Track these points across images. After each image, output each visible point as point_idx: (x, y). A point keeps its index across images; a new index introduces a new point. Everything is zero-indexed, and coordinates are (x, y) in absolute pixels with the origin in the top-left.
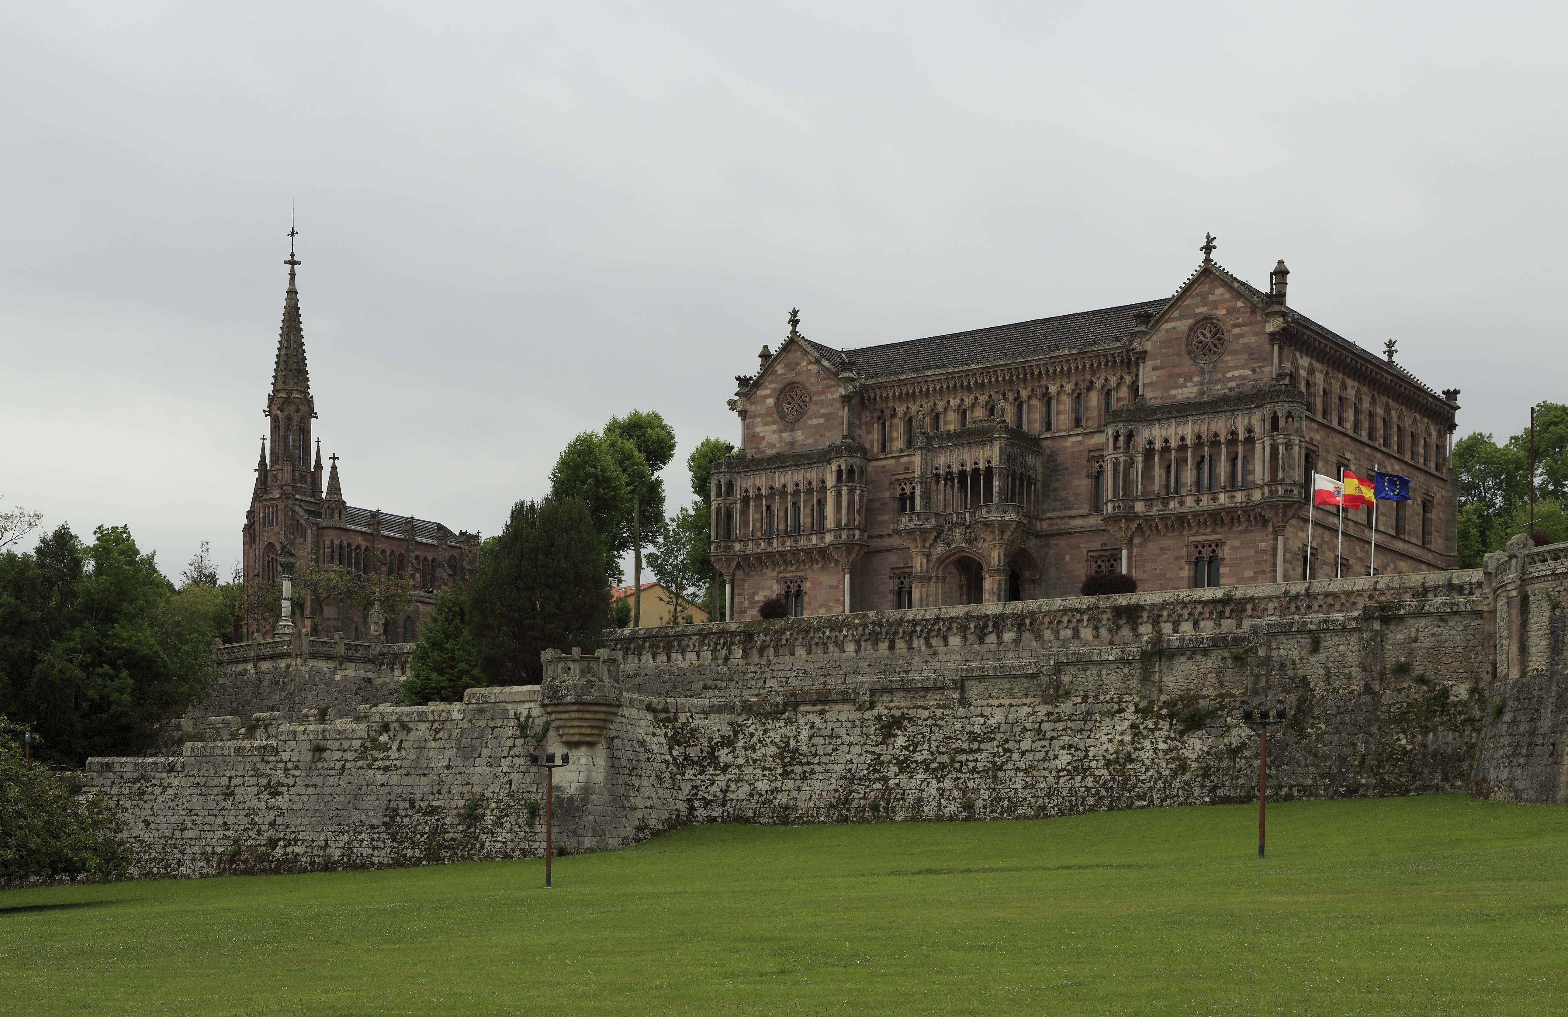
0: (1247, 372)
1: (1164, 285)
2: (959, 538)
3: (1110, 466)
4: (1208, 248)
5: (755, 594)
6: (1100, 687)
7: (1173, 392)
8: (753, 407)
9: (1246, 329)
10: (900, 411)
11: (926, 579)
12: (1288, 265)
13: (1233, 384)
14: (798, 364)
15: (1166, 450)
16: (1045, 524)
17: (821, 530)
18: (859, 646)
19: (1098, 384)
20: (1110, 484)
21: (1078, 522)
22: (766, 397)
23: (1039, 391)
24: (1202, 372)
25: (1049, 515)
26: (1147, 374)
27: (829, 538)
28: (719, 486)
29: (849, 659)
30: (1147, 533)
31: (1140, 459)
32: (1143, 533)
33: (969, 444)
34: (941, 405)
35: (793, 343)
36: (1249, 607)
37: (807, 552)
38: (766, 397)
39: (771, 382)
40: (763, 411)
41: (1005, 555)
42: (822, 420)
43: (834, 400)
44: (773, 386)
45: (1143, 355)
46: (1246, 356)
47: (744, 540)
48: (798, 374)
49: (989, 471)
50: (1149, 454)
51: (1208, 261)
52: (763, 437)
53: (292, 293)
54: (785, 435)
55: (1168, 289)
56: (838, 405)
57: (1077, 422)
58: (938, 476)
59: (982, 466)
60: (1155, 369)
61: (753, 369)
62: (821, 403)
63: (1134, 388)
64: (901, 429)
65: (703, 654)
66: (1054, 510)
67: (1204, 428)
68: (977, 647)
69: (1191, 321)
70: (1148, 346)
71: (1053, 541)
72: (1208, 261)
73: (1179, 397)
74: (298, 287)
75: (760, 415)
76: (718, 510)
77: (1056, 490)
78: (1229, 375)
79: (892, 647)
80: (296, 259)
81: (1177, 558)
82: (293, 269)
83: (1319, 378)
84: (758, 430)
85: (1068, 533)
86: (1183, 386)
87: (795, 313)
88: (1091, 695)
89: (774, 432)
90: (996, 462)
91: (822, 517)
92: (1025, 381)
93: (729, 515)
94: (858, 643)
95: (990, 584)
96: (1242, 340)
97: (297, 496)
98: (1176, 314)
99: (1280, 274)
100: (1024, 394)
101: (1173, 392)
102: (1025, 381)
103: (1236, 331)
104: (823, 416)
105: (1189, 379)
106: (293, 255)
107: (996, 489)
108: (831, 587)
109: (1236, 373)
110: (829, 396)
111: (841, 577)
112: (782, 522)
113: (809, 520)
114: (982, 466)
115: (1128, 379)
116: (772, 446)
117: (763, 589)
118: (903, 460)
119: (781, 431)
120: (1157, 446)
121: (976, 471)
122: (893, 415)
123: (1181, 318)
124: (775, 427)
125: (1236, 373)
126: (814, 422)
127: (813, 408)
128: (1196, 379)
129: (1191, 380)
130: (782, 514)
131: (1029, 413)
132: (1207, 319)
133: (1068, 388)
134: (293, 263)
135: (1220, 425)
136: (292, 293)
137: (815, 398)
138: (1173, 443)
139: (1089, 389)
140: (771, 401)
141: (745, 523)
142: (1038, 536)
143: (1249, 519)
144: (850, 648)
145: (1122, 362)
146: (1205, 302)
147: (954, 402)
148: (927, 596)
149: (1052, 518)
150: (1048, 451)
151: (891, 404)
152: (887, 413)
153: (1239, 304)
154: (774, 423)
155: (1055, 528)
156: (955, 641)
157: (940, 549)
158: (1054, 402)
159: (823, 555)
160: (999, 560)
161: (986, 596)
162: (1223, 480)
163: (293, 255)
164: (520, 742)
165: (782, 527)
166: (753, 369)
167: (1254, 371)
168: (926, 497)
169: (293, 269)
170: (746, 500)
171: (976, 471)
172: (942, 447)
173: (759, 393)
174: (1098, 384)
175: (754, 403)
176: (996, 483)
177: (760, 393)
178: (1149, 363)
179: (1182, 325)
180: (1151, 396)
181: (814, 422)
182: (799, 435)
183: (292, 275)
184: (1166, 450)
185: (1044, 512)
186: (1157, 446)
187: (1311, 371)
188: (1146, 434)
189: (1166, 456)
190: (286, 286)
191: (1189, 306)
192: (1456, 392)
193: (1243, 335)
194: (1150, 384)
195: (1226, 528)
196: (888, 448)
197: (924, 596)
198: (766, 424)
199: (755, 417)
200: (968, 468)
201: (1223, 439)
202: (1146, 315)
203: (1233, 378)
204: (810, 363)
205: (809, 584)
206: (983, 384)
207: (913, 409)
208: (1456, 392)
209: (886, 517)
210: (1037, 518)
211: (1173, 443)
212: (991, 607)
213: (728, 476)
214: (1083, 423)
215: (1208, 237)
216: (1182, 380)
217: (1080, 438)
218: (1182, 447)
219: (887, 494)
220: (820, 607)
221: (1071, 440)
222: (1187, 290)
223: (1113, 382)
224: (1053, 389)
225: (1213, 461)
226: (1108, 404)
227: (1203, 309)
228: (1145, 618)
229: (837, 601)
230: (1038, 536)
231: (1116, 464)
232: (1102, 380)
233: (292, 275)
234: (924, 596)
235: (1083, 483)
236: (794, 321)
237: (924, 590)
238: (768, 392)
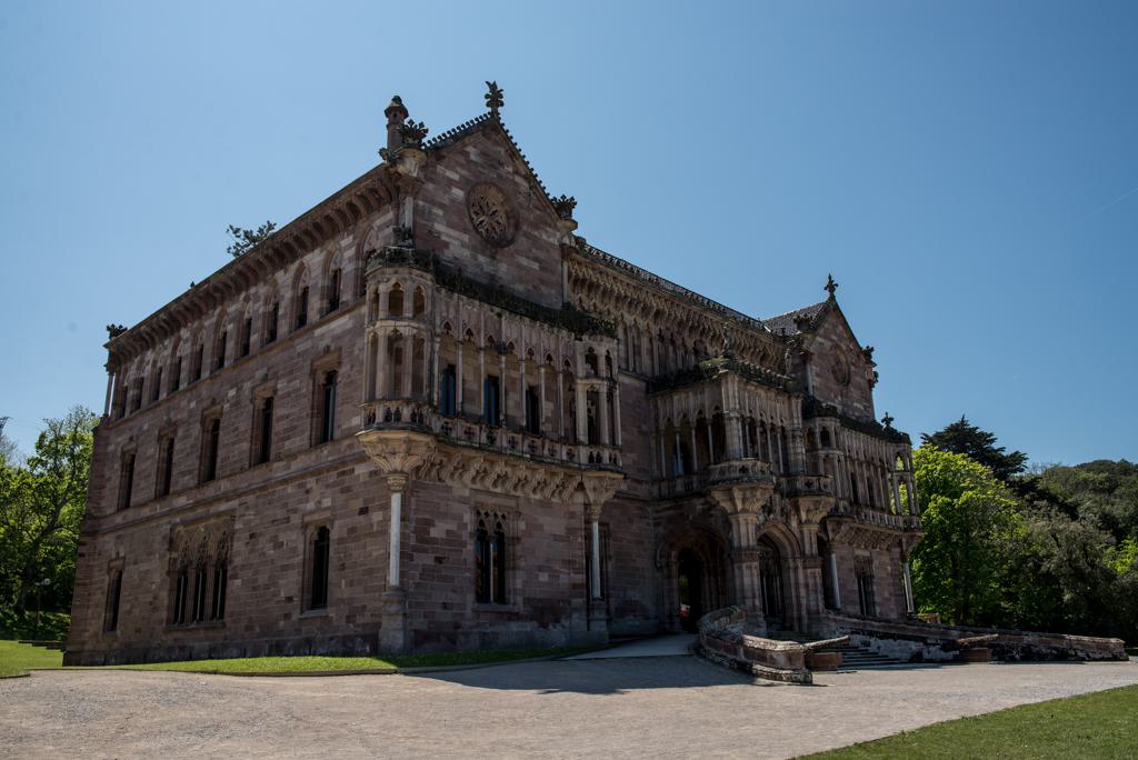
2: (778, 509)
4: (831, 287)
5: (430, 523)
8: (430, 186)
14: (502, 164)
38: (451, 183)
39: (462, 166)
40: (446, 202)
42: (536, 266)
43: (552, 245)
44: (464, 172)
48: (500, 176)
52: (446, 245)
54: (481, 258)
56: (556, 255)
60: (818, 375)
62: (535, 241)
72: (832, 298)
75: (442, 206)
84: (439, 227)
89: (463, 245)
104: (536, 259)
108: (556, 538)
109: (858, 405)
110: (544, 237)
117: (445, 516)
124: (466, 238)
126: (524, 261)
137: (525, 228)
154: (465, 231)
167: (865, 407)
173: (440, 168)
175: (432, 181)
181: (524, 261)
198: (450, 225)
199: (433, 203)
204: (516, 172)
205: (522, 526)
215: (830, 278)
216: (832, 395)
220: (541, 569)
238: (456, 177)
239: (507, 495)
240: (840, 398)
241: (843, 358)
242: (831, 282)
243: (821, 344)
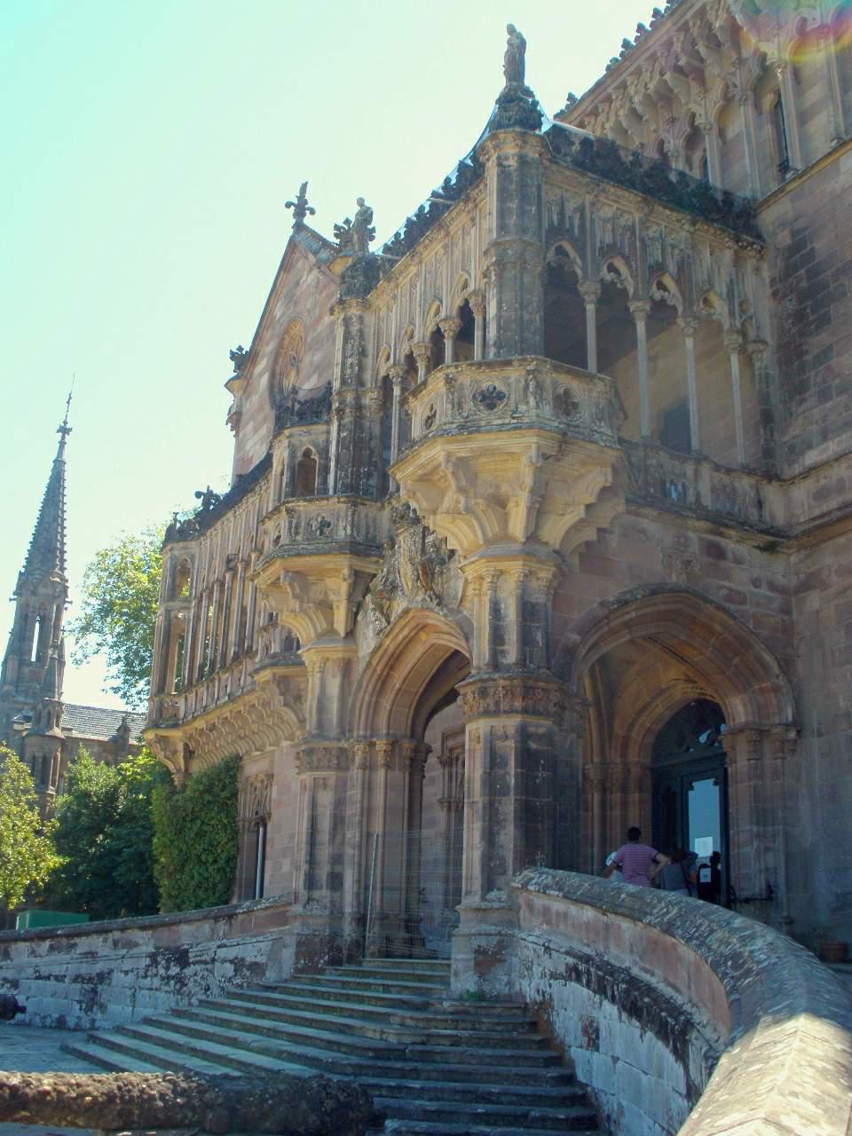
16: (801, 492)
22: (261, 375)
25: (812, 457)
41: (527, 610)
53: (59, 465)
66: (825, 436)
71: (827, 559)
74: (65, 457)
77: (826, 353)
80: (68, 426)
82: (63, 437)
97: (21, 699)
106: (65, 423)
134: (64, 430)
136: (59, 465)
140: (265, 380)
142: (774, 540)
148: (338, 822)
149: (825, 464)
150: (784, 238)
155: (833, 503)
160: (497, 637)
163: (65, 423)
169: (63, 437)
183: (62, 444)
185: (795, 451)
190: (54, 456)
197: (325, 825)
210: (771, 476)
230: (774, 540)
233: (62, 444)
234: (325, 825)
237: (326, 798)
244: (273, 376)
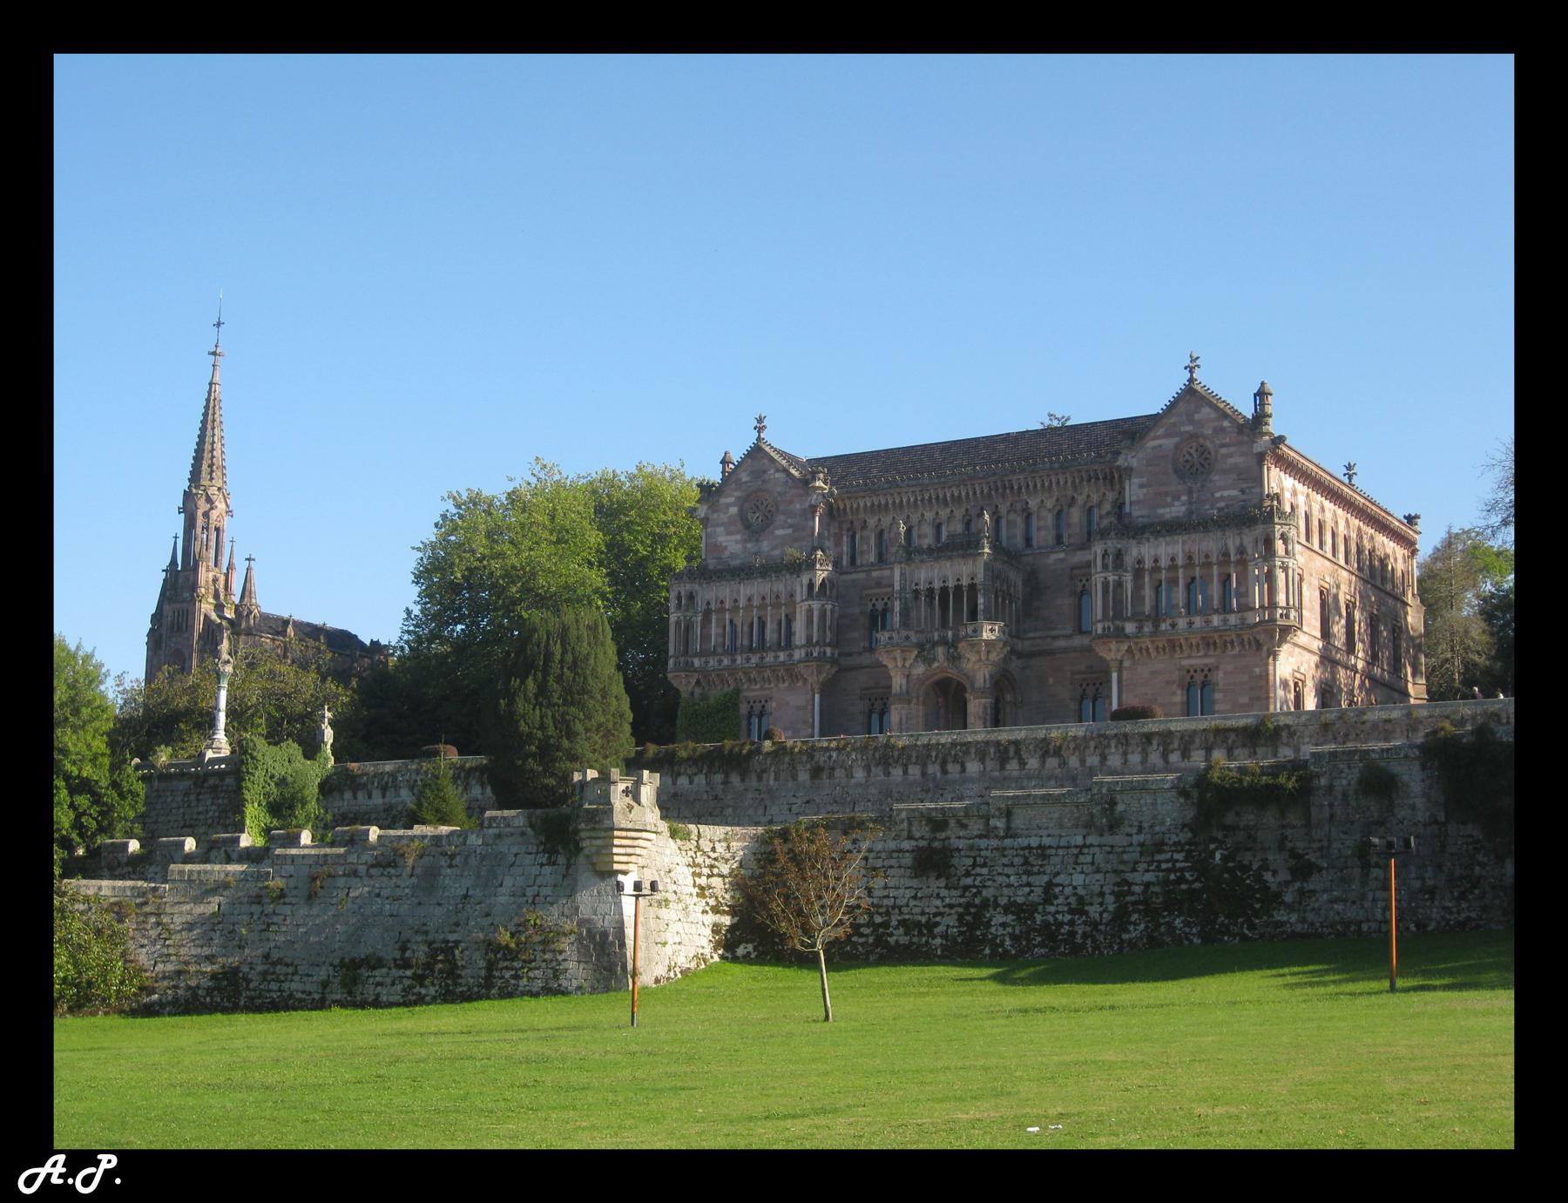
0: (1235, 493)
1: (1152, 404)
3: (1099, 586)
6: (1155, 817)
7: (1161, 511)
9: (1232, 449)
10: (872, 522)
11: (905, 698)
12: (1269, 387)
13: (1222, 504)
15: (1156, 569)
16: (1027, 643)
17: (789, 645)
18: (869, 771)
19: (1080, 500)
20: (1100, 603)
21: (1061, 643)
23: (1019, 506)
24: (1190, 492)
26: (1134, 491)
27: (798, 654)
28: (679, 598)
29: (859, 785)
30: (1137, 656)
31: (1128, 578)
32: (1133, 656)
33: (950, 558)
34: (915, 518)
35: (757, 452)
36: (1284, 734)
37: (774, 668)
38: (729, 505)
42: (790, 531)
44: (738, 494)
45: (1129, 471)
46: (1234, 476)
47: (703, 654)
49: (972, 588)
50: (1138, 574)
51: (1191, 380)
55: (1154, 406)
57: (1059, 539)
58: (917, 592)
59: (965, 582)
60: (1141, 486)
61: (716, 477)
63: (1119, 505)
64: (872, 542)
65: (696, 779)
67: (1195, 549)
68: (997, 774)
69: (1177, 439)
70: (1134, 463)
73: (1168, 516)
76: (678, 623)
78: (1218, 495)
79: (905, 772)
81: (1169, 683)
83: (1301, 500)
84: (720, 539)
85: (1051, 653)
86: (1170, 505)
87: (760, 420)
88: (1146, 825)
90: (980, 578)
91: (790, 634)
92: (1003, 495)
93: (689, 627)
94: (868, 768)
95: (976, 706)
96: (1231, 461)
98: (1161, 432)
99: (1261, 395)
100: (1003, 509)
101: (1161, 511)
102: (1003, 495)
103: (1224, 451)
105: (1178, 498)
107: (981, 607)
108: (798, 708)
109: (1226, 493)
111: (809, 696)
112: (746, 636)
113: (775, 636)
114: (965, 582)
115: (1111, 496)
116: (733, 556)
118: (875, 574)
119: (745, 541)
120: (1148, 564)
121: (958, 588)
122: (864, 526)
123: (1167, 435)
124: (738, 537)
125: (1226, 493)
126: (779, 532)
127: (780, 518)
128: (1184, 498)
129: (1178, 498)
130: (746, 628)
131: (1008, 528)
132: (1193, 437)
133: (1049, 504)
135: (1209, 544)
138: (1164, 563)
139: (1070, 505)
140: (734, 510)
141: (706, 638)
143: (1242, 643)
144: (859, 775)
145: (1105, 478)
146: (1191, 421)
147: (929, 515)
151: (862, 515)
152: (857, 525)
153: (1226, 424)
156: (973, 767)
157: (920, 670)
158: (1034, 518)
159: (791, 673)
161: (971, 719)
162: (1216, 602)
164: (547, 869)
165: (746, 642)
166: (716, 477)
167: (1243, 491)
168: (905, 613)
170: (707, 613)
171: (958, 588)
172: (922, 561)
174: (1080, 500)
176: (981, 600)
177: (723, 501)
178: (1135, 481)
179: (1169, 443)
180: (1137, 513)
181: (779, 532)
182: (765, 546)
184: (1156, 569)
186: (1148, 564)
187: (1294, 493)
188: (1135, 552)
189: (1156, 576)
191: (1174, 424)
192: (1417, 517)
193: (1231, 456)
194: (1138, 502)
195: (1219, 652)
196: (858, 562)
198: (729, 534)
200: (951, 584)
201: (1214, 560)
202: (1131, 430)
203: (1222, 498)
204: (777, 471)
206: (960, 497)
207: (887, 521)
208: (1417, 517)
209: (856, 635)
211: (1164, 563)
212: (977, 732)
213: (688, 586)
214: (1065, 540)
217: (1062, 555)
218: (1173, 567)
219: (857, 610)
221: (1054, 557)
222: (1173, 405)
223: (1095, 498)
224: (1033, 503)
225: (1207, 580)
226: (1089, 523)
227: (1189, 428)
228: (1176, 745)
229: (805, 722)
231: (1106, 585)
232: (1084, 496)
235: (1065, 603)
236: (760, 429)
239: (762, 688)
240: (1184, 498)
241: (1208, 444)
242: (1193, 360)
243: (1154, 448)
244: (741, 510)
